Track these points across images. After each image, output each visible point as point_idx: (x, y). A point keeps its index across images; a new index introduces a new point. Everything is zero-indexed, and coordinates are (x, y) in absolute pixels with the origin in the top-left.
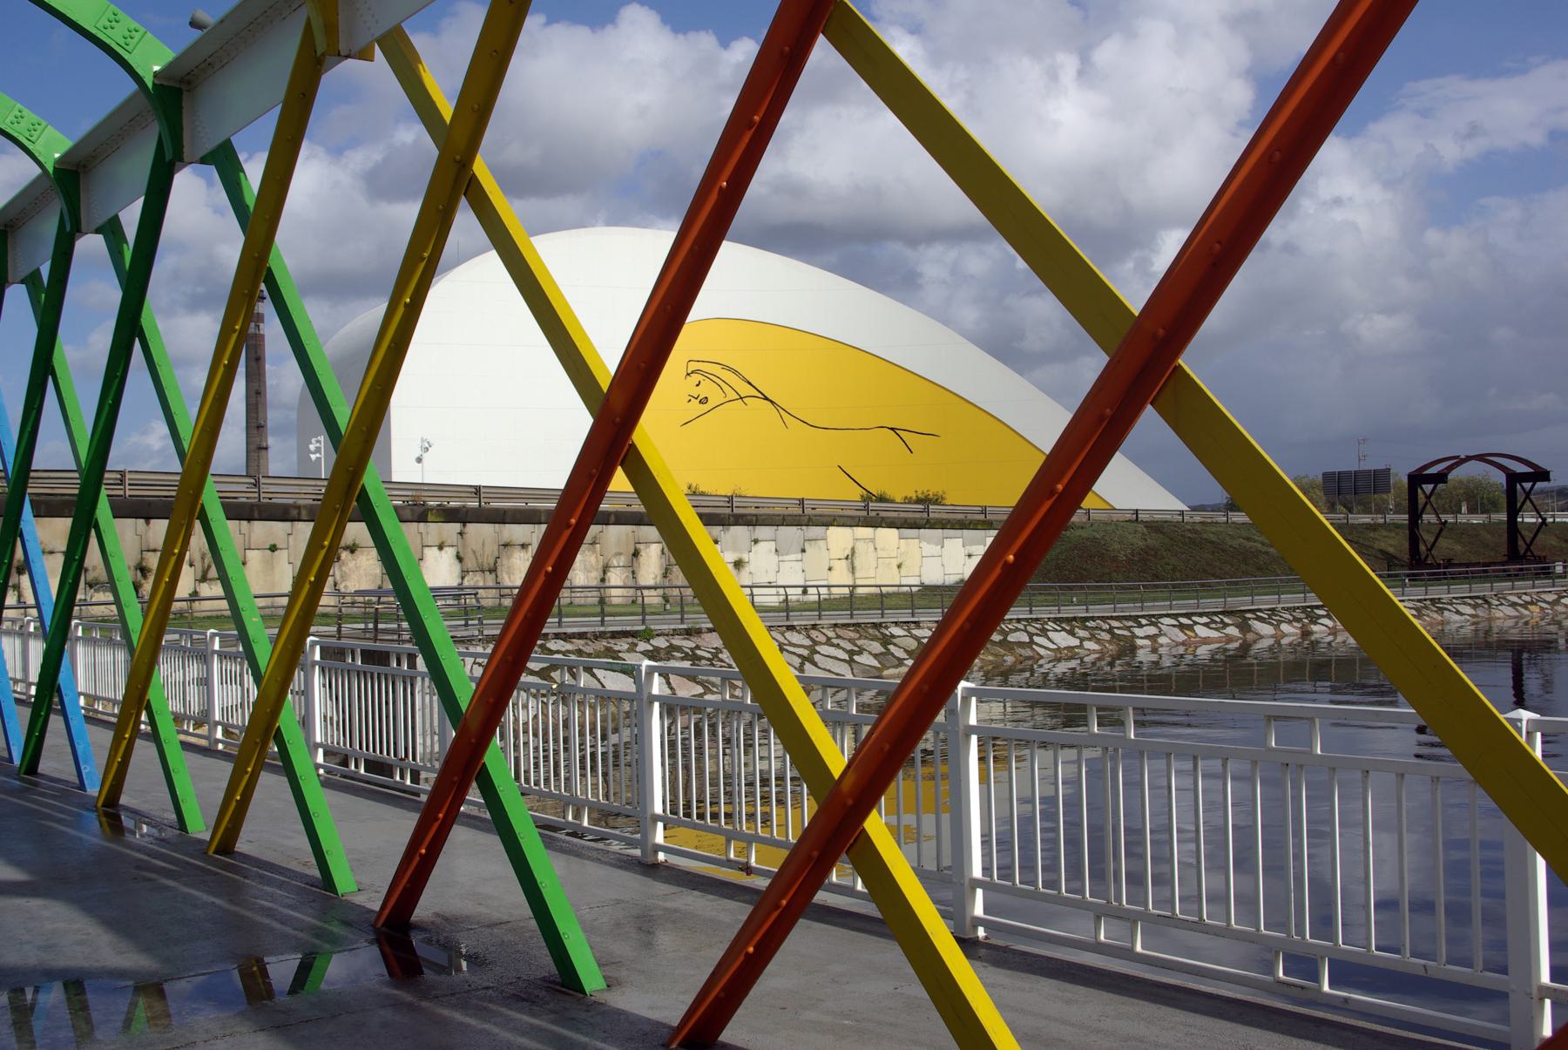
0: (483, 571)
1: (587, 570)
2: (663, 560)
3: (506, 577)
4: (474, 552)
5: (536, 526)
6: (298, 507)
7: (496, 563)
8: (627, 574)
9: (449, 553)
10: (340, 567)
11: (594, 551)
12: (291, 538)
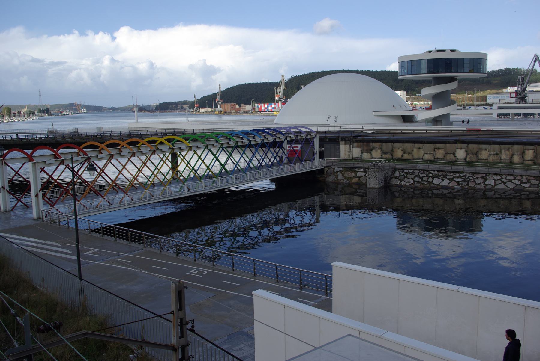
0: (473, 154)
1: (506, 155)
2: (535, 154)
3: (480, 155)
4: (471, 150)
5: (490, 145)
6: (424, 141)
7: (477, 152)
8: (520, 156)
9: (463, 150)
10: (435, 152)
11: (509, 151)
12: (423, 147)
